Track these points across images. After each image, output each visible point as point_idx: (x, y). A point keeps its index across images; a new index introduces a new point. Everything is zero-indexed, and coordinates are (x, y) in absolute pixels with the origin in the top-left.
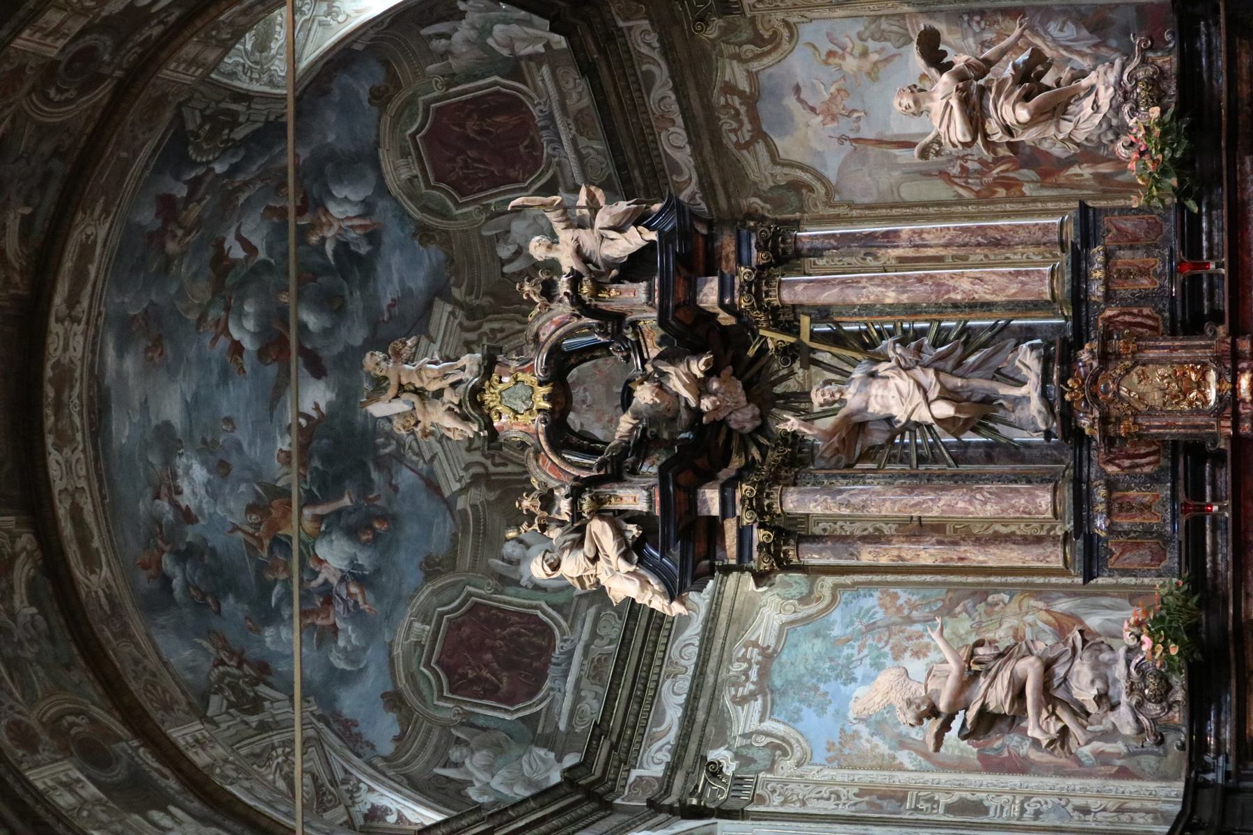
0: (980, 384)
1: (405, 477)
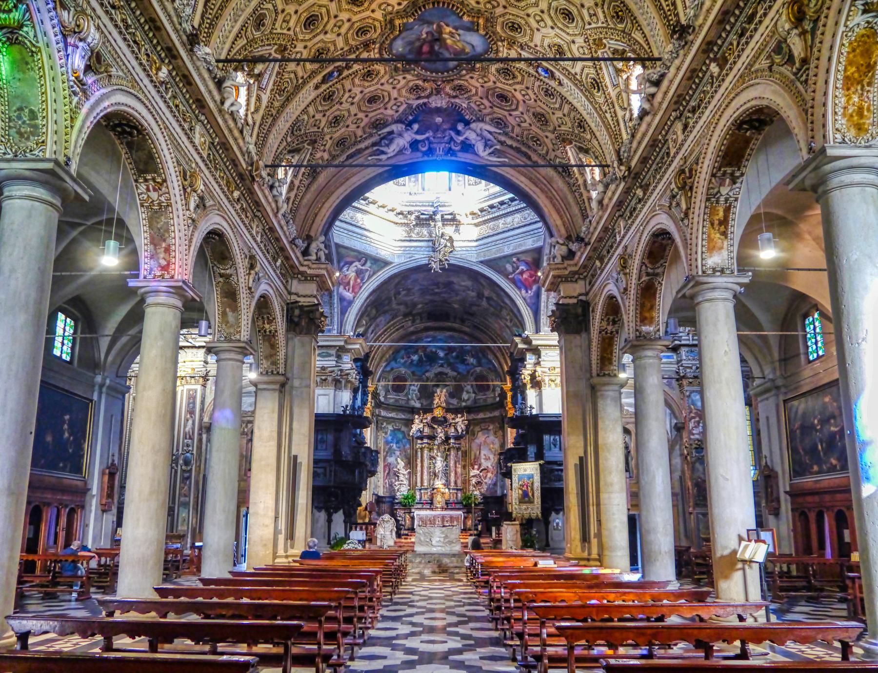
0: (440, 475)
1: (428, 368)
